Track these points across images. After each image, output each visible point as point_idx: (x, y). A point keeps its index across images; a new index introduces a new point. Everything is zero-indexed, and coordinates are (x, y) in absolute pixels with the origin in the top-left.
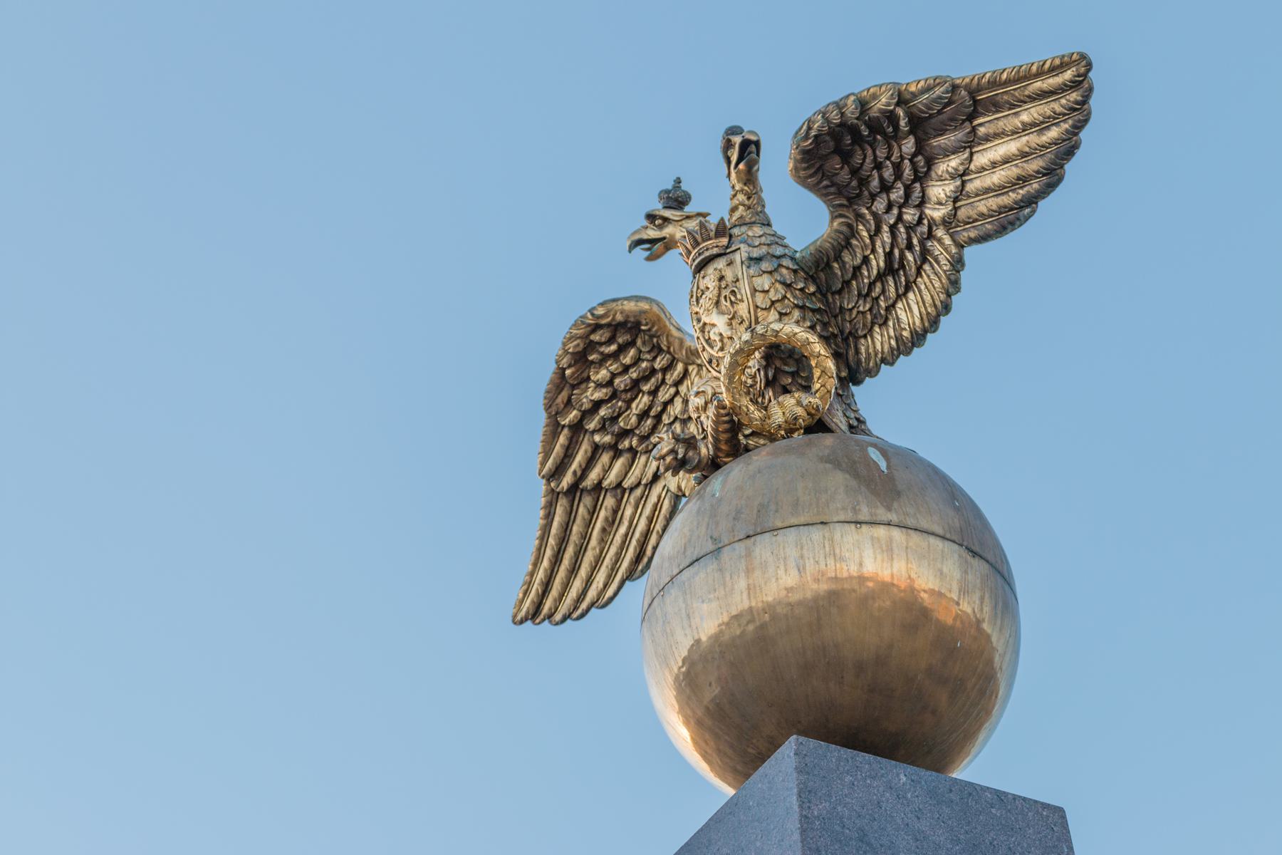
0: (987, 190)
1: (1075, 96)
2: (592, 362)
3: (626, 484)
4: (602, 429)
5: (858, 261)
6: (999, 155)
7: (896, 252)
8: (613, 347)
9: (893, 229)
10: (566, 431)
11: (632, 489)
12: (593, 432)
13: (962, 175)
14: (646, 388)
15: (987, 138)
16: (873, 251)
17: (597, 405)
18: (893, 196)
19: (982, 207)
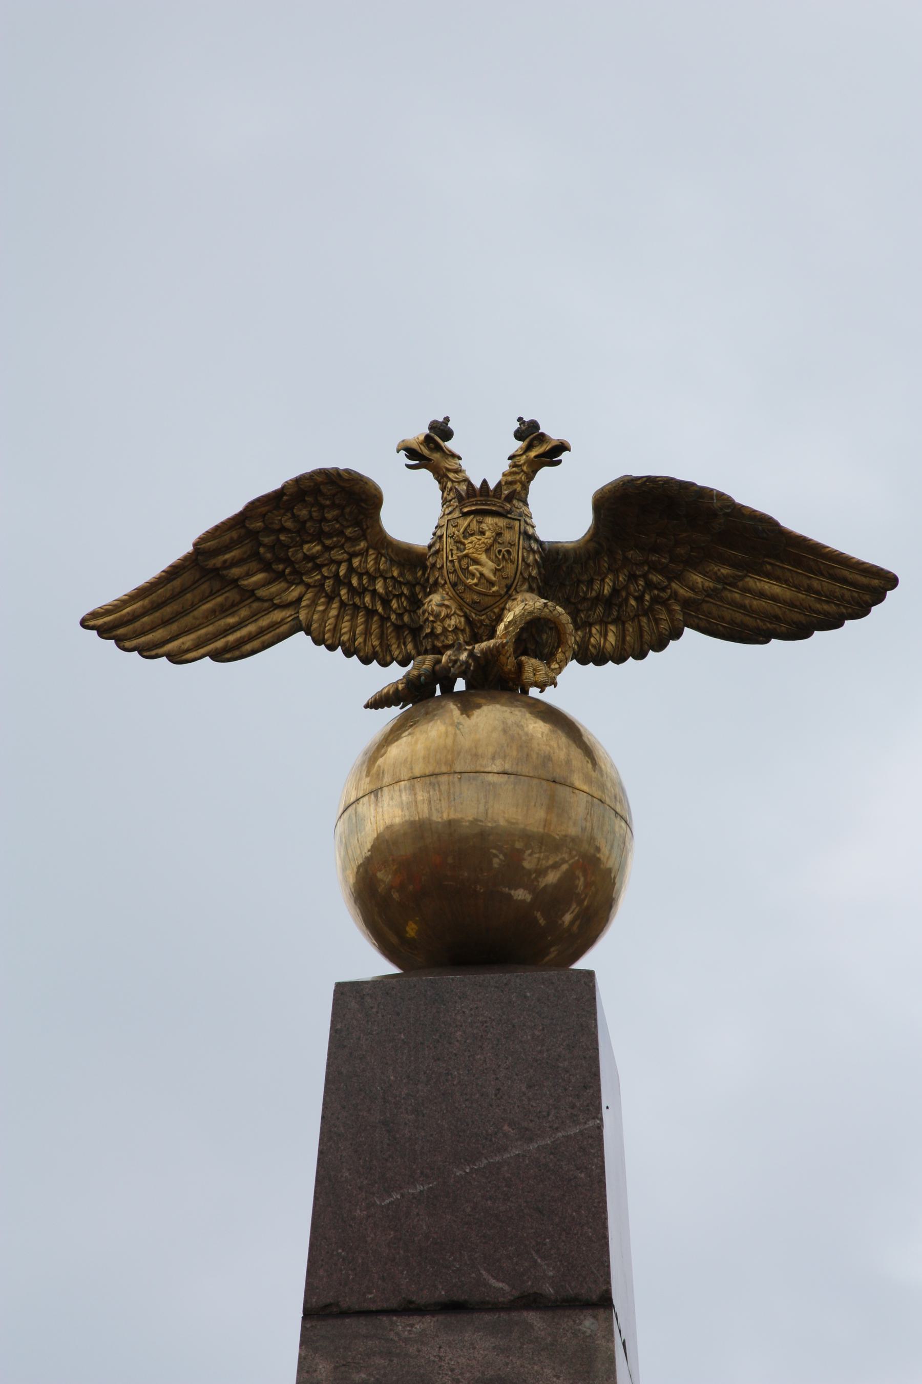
0: (742, 607)
1: (867, 597)
2: (304, 501)
3: (261, 593)
4: (271, 548)
5: (585, 578)
7: (624, 594)
8: (328, 502)
9: (633, 577)
10: (243, 531)
11: (259, 599)
12: (264, 546)
14: (328, 542)
15: (768, 575)
16: (603, 580)
17: (283, 529)
18: (654, 558)
19: (728, 614)
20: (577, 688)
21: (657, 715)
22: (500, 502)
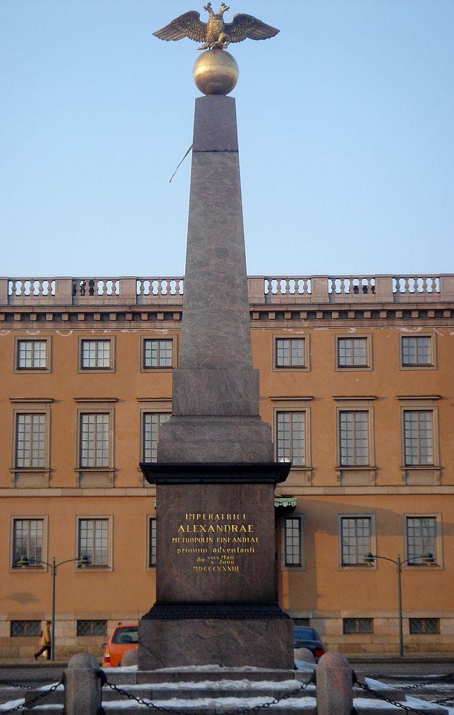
20: (232, 48)
21: (243, 51)
22: (220, 17)
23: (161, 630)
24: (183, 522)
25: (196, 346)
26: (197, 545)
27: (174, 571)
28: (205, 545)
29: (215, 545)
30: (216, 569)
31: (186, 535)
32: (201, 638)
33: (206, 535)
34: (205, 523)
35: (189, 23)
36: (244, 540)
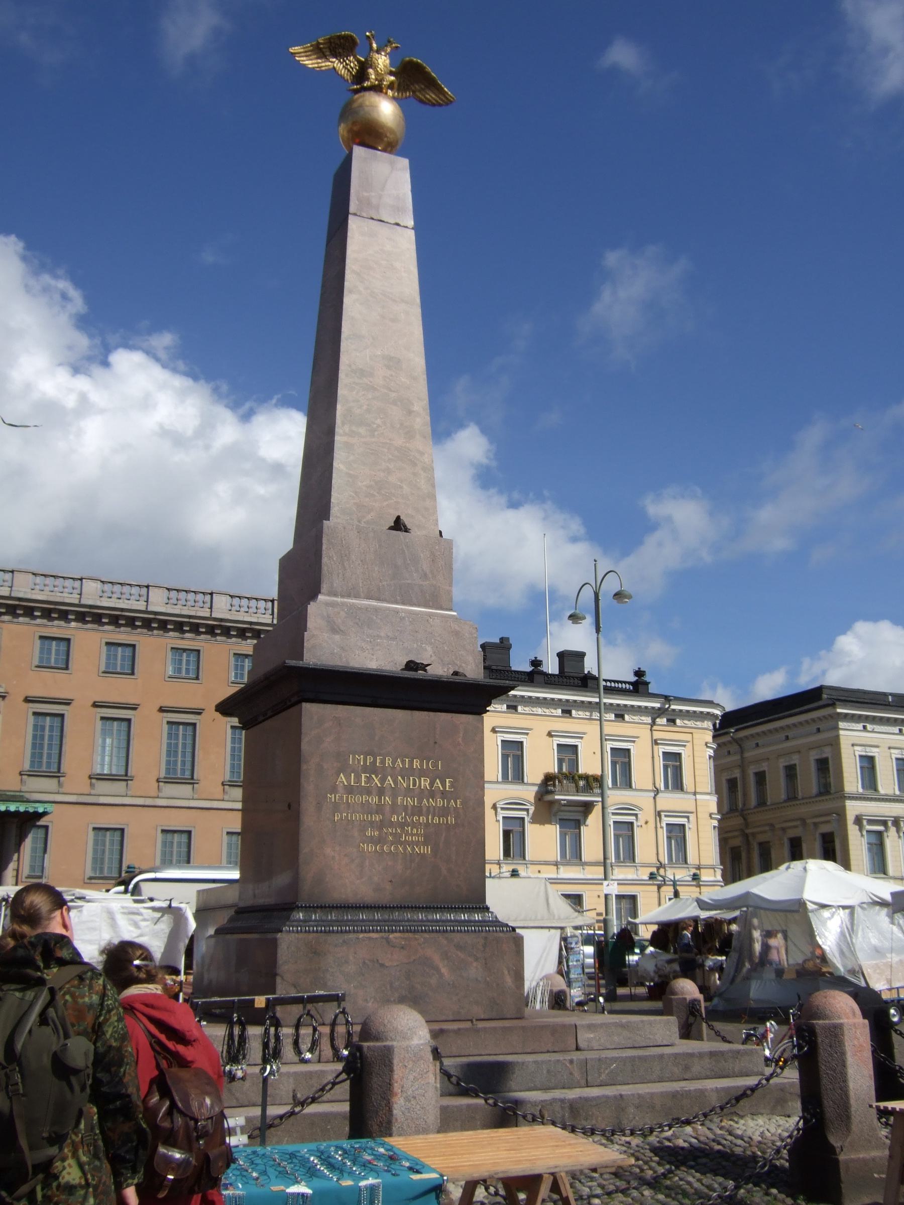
6: (431, 96)
13: (423, 90)
23: (315, 953)
24: (344, 768)
25: (356, 493)
26: (366, 808)
27: (328, 851)
28: (380, 809)
29: (394, 808)
30: (396, 848)
31: (350, 790)
32: (382, 965)
33: (381, 792)
34: (382, 772)
35: (340, 50)
36: (440, 802)
